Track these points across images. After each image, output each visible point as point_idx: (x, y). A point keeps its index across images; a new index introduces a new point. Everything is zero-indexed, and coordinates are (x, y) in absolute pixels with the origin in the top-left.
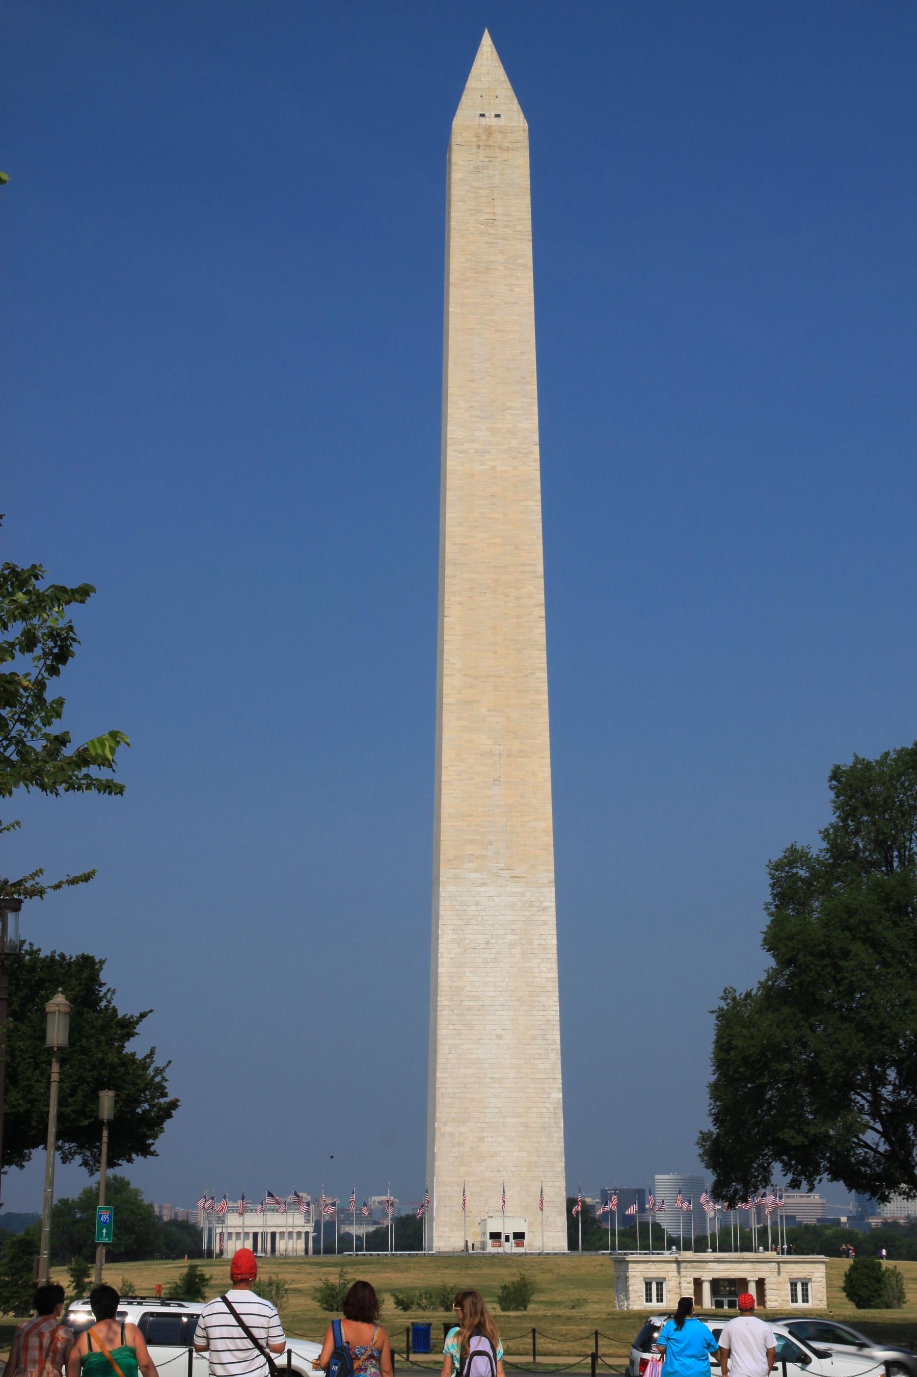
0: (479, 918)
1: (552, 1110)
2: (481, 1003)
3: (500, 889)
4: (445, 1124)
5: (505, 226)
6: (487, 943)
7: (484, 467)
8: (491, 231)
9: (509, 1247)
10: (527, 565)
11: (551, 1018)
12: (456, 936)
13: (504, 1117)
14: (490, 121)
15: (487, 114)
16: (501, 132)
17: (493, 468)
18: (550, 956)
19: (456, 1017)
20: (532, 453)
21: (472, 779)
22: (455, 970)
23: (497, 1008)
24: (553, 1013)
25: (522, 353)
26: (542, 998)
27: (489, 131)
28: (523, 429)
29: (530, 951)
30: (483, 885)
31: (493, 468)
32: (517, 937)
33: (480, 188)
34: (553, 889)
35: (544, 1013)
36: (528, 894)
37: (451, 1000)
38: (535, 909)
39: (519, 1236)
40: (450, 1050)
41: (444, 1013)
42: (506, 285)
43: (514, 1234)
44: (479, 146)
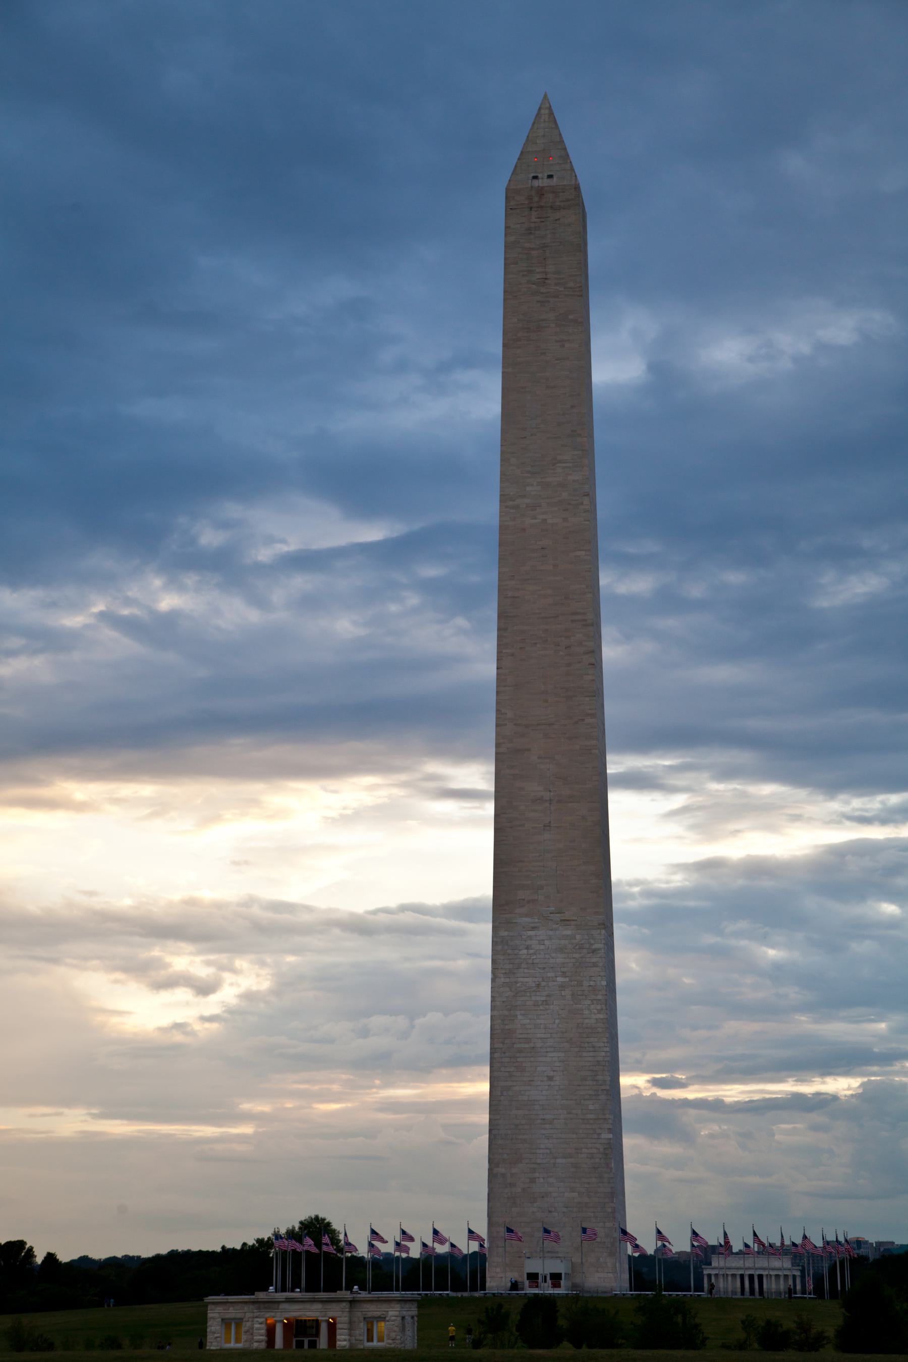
0: (530, 961)
1: (602, 1150)
2: (532, 1045)
3: (551, 933)
5: (556, 284)
6: (538, 986)
7: (536, 521)
8: (543, 290)
9: (547, 1289)
11: (600, 1059)
12: (507, 980)
13: (556, 1158)
14: (543, 182)
15: (540, 176)
16: (553, 192)
17: (544, 521)
18: (600, 997)
19: (507, 1060)
20: (582, 504)
22: (507, 1013)
23: (549, 1050)
24: (603, 1054)
25: (572, 407)
26: (592, 1039)
27: (541, 192)
28: (574, 481)
29: (579, 993)
30: (533, 928)
31: (544, 521)
32: (567, 979)
33: (533, 249)
36: (578, 937)
37: (503, 1043)
38: (585, 951)
39: (556, 1278)
41: (496, 1055)
42: (557, 341)
43: (551, 1274)
44: (531, 208)
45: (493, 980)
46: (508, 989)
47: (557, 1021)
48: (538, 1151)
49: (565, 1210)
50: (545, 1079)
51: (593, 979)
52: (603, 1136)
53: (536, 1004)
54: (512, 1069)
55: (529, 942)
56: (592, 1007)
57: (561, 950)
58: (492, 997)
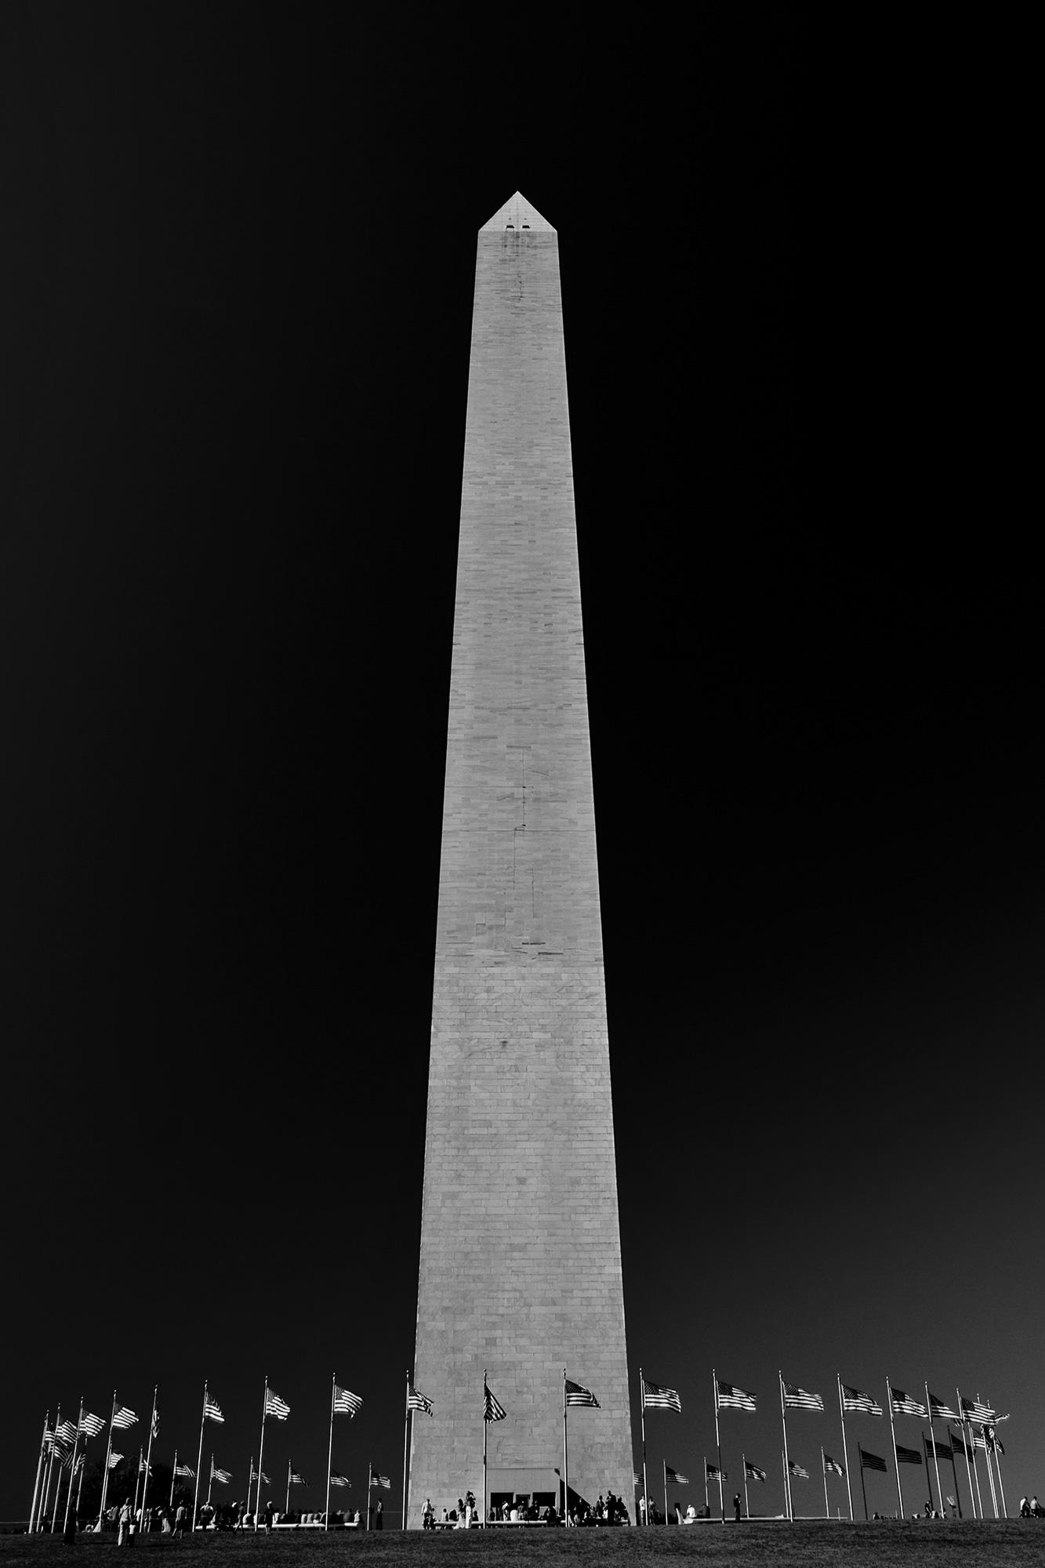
1: (606, 1293)
2: (492, 1131)
3: (524, 970)
4: (433, 1316)
10: (559, 590)
18: (599, 1061)
19: (453, 1152)
21: (485, 829)
22: (454, 1083)
23: (519, 1137)
24: (605, 1144)
27: (517, 236)
34: (602, 969)
35: (593, 1144)
36: (564, 976)
37: (447, 1126)
38: (576, 996)
40: (443, 1203)
41: (435, 1145)
46: (456, 1048)
47: (533, 1096)
48: (500, 1294)
49: (545, 1390)
50: (515, 1181)
51: (588, 1035)
52: (607, 1270)
53: (501, 1071)
54: (461, 1166)
55: (491, 983)
56: (588, 1075)
57: (538, 993)
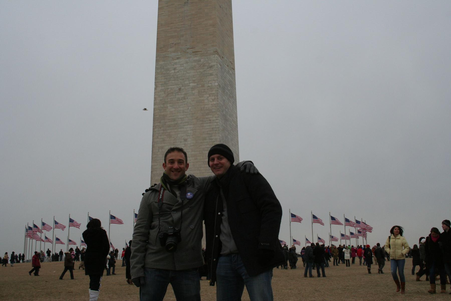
6: (180, 89)
12: (163, 88)
18: (214, 92)
22: (162, 106)
24: (215, 124)
30: (178, 58)
32: (196, 84)
36: (202, 60)
37: (160, 122)
38: (206, 67)
41: (156, 130)
45: (155, 89)
47: (190, 108)
51: (210, 82)
55: (175, 66)
58: (155, 98)
